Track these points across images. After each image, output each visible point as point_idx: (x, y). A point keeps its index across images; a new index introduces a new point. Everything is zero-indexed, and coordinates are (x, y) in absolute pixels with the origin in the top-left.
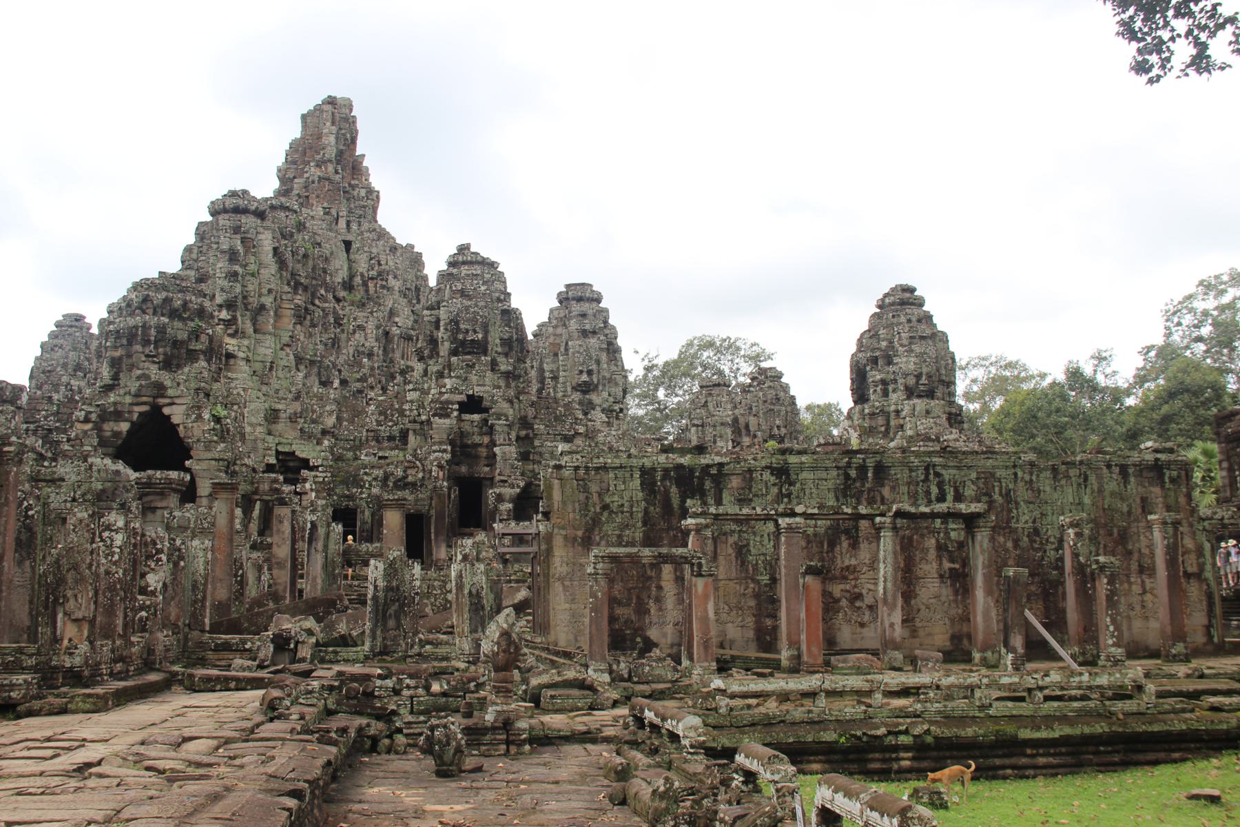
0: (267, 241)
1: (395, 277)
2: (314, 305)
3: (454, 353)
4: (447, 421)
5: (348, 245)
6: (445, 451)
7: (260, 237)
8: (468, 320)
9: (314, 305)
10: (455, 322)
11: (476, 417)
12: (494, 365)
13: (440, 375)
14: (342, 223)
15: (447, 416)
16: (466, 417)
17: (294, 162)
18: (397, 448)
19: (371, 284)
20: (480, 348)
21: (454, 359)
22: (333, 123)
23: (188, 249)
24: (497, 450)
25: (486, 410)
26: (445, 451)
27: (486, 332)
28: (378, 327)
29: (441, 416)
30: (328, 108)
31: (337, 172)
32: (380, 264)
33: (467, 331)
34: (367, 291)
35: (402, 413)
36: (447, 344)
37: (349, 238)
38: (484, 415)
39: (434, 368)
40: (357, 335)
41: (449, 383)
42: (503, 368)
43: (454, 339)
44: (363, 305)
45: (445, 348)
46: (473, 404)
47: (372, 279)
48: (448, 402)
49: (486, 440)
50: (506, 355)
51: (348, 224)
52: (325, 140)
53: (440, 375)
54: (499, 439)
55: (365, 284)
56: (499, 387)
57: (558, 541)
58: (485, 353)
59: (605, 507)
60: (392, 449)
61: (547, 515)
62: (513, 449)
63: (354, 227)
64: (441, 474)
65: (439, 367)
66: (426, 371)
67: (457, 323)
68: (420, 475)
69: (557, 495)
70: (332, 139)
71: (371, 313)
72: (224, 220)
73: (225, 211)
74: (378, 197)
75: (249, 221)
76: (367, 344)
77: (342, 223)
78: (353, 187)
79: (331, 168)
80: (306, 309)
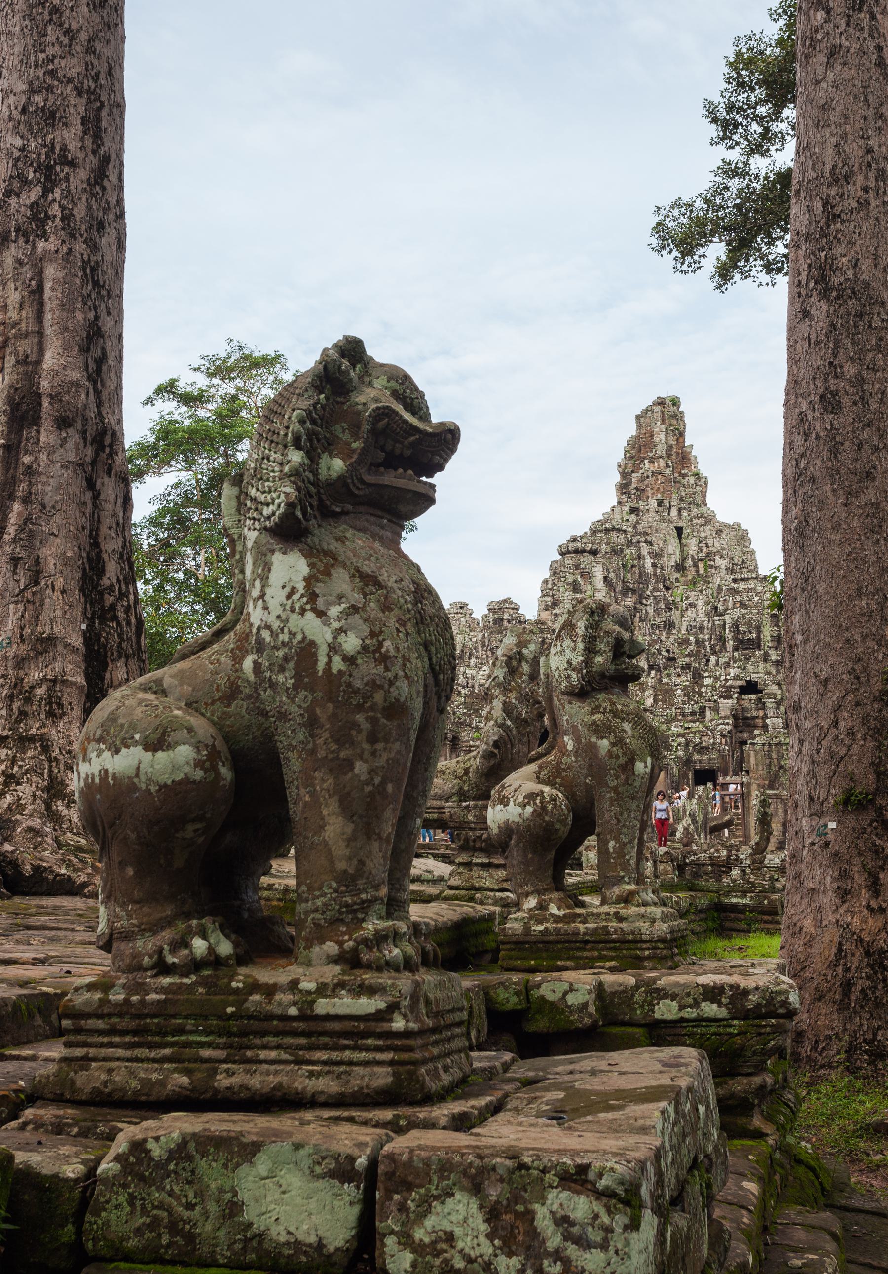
0: (598, 572)
1: (722, 557)
2: (642, 604)
3: (736, 649)
4: (730, 701)
5: (679, 530)
6: (728, 724)
7: (594, 569)
8: (745, 624)
9: (642, 604)
10: (736, 626)
11: (753, 697)
12: (766, 658)
13: (727, 665)
14: (674, 512)
15: (730, 697)
16: (745, 696)
17: (631, 458)
18: (697, 720)
19: (701, 565)
20: (756, 644)
21: (736, 654)
22: (663, 422)
23: (546, 582)
24: (768, 721)
25: (760, 691)
26: (728, 724)
27: (759, 632)
28: (707, 603)
29: (725, 698)
30: (657, 409)
31: (667, 466)
32: (707, 547)
33: (745, 632)
34: (697, 571)
35: (700, 694)
36: (731, 642)
37: (680, 524)
38: (759, 695)
39: (722, 661)
40: (689, 612)
41: (733, 672)
42: (774, 658)
43: (735, 639)
44: (695, 583)
45: (730, 644)
46: (751, 687)
47: (701, 560)
48: (732, 687)
49: (761, 713)
50: (776, 648)
51: (680, 510)
52: (656, 439)
53: (727, 665)
54: (770, 713)
55: (695, 565)
56: (769, 674)
57: (754, 787)
58: (759, 648)
59: (781, 767)
60: (694, 722)
61: (748, 772)
62: (780, 720)
63: (685, 513)
64: (724, 741)
65: (726, 660)
66: (717, 662)
67: (737, 627)
68: (712, 741)
69: (753, 760)
70: (662, 436)
71: (701, 591)
72: (569, 561)
73: (569, 553)
74: (706, 483)
75: (586, 559)
76: (698, 619)
77: (674, 512)
78: (684, 476)
79: (662, 463)
80: (635, 608)
